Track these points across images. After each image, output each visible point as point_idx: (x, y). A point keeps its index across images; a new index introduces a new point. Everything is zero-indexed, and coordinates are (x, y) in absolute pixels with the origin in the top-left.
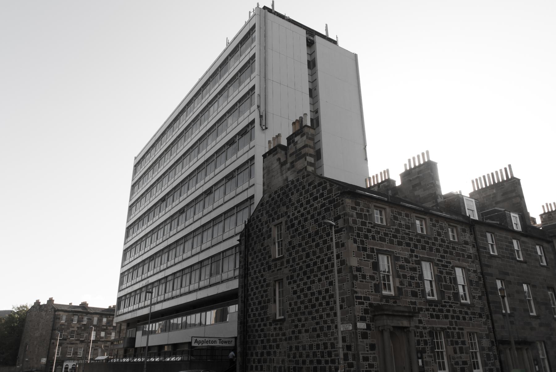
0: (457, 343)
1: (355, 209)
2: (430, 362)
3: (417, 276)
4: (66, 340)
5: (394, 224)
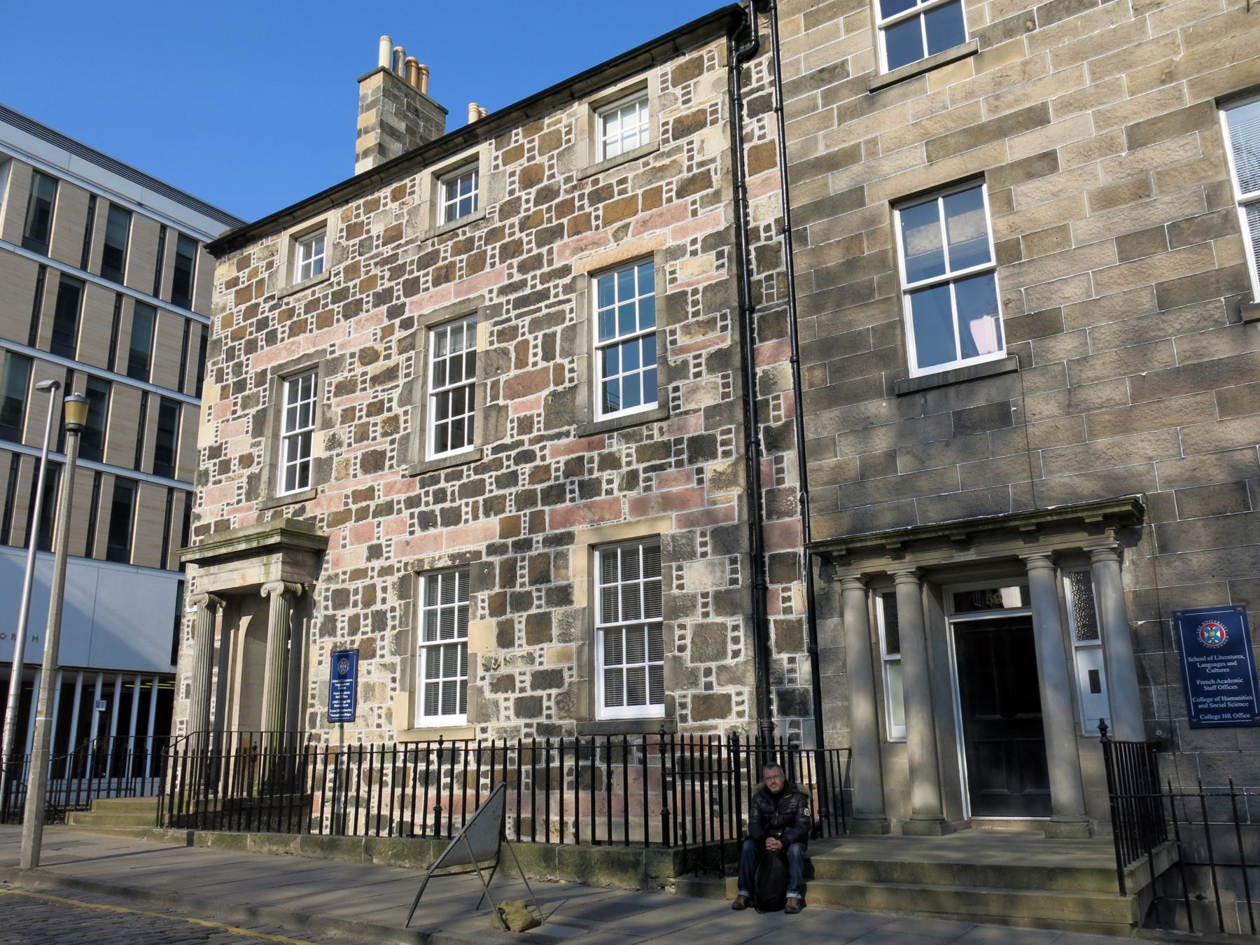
0: (522, 602)
3: (396, 394)
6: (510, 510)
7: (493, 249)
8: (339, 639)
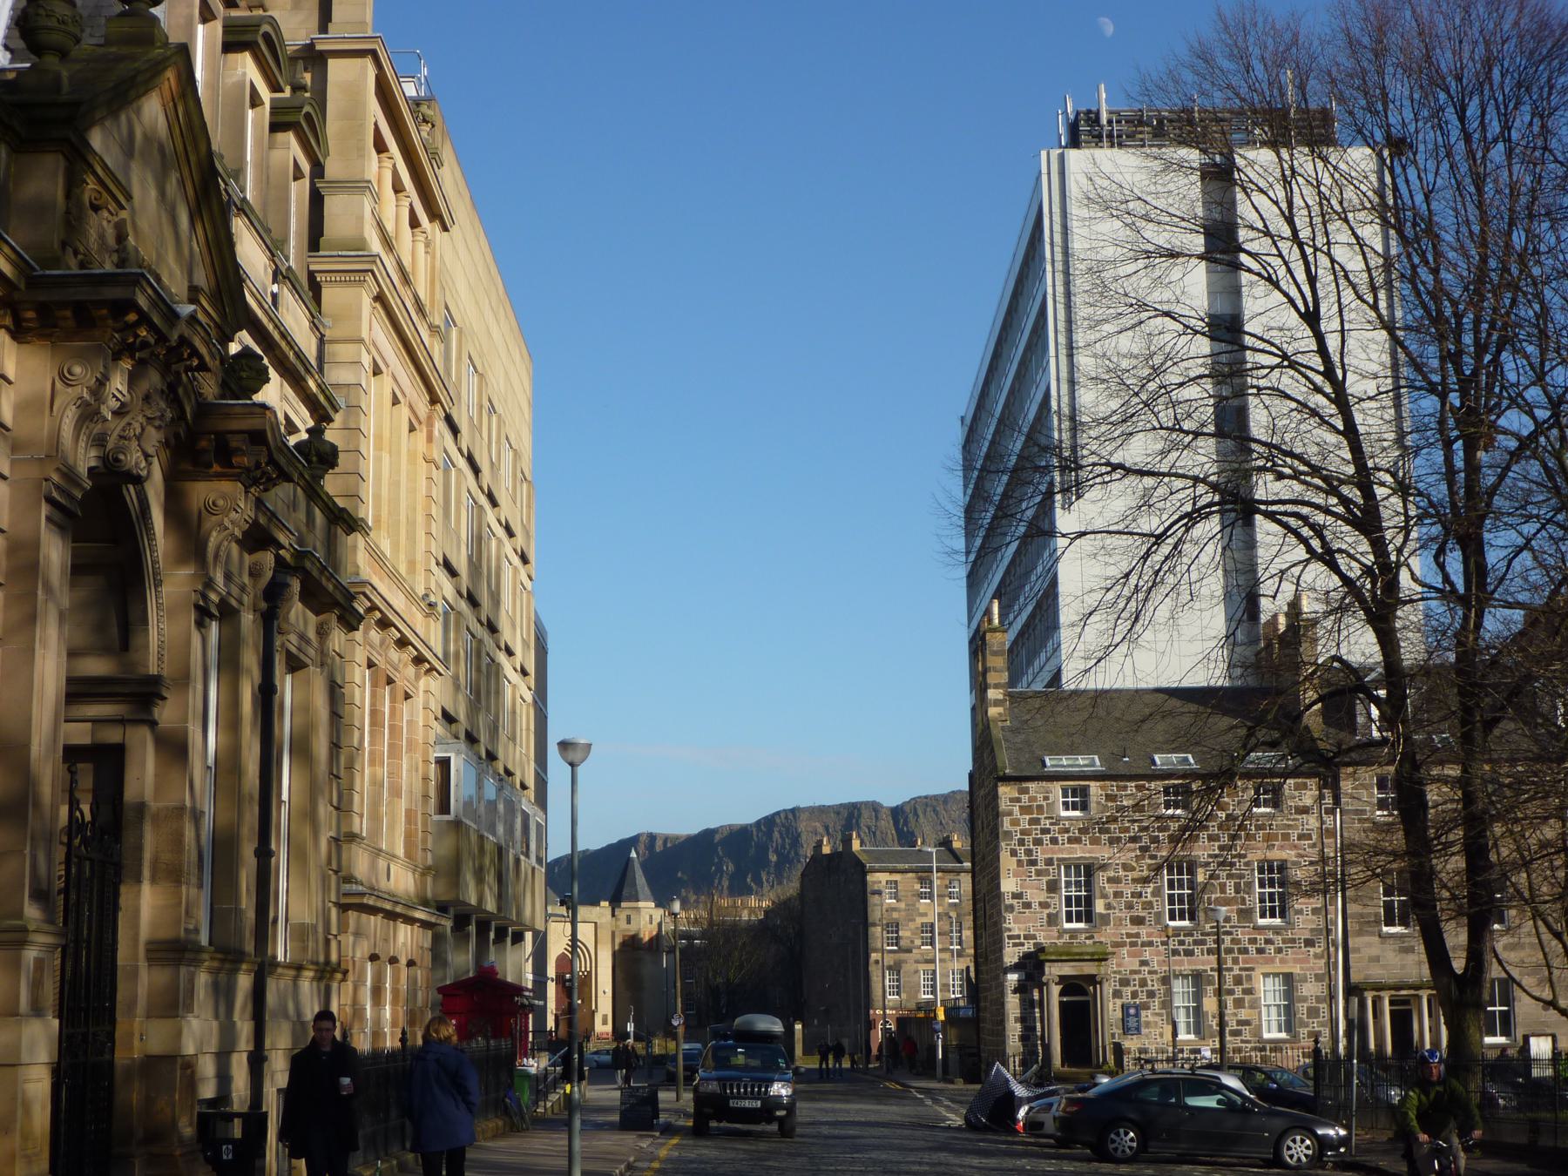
1: (1018, 800)
4: (909, 951)
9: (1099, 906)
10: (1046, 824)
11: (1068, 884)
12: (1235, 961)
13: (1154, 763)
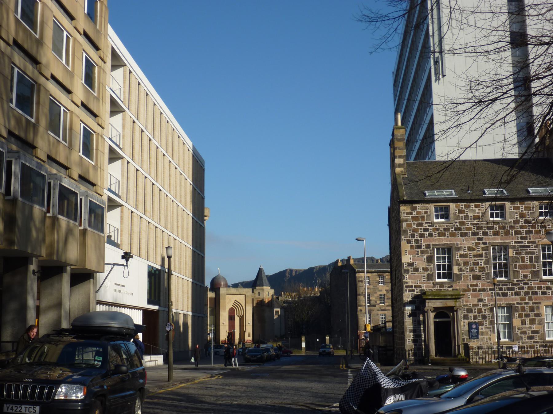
0: (527, 316)
1: (411, 213)
2: (487, 332)
3: (483, 261)
4: (375, 306)
5: (458, 218)
6: (522, 295)
7: (512, 231)
8: (470, 320)
9: (456, 270)
10: (426, 226)
11: (438, 258)
12: (530, 299)
13: (484, 193)
